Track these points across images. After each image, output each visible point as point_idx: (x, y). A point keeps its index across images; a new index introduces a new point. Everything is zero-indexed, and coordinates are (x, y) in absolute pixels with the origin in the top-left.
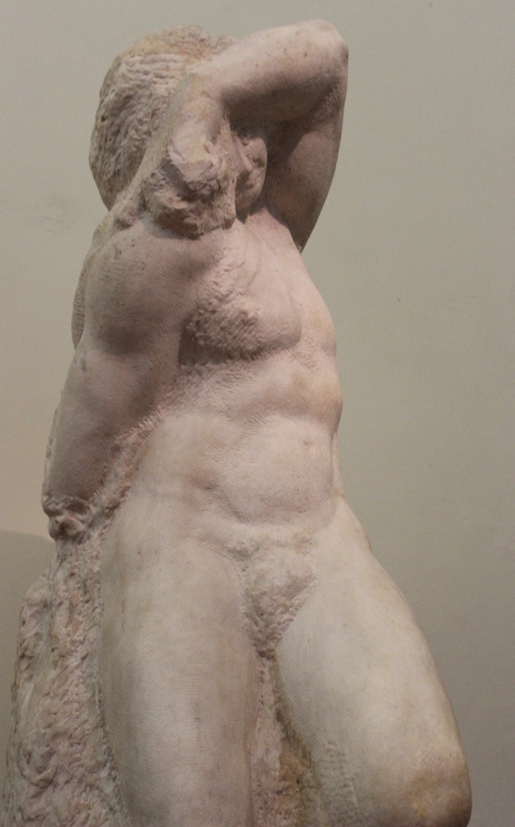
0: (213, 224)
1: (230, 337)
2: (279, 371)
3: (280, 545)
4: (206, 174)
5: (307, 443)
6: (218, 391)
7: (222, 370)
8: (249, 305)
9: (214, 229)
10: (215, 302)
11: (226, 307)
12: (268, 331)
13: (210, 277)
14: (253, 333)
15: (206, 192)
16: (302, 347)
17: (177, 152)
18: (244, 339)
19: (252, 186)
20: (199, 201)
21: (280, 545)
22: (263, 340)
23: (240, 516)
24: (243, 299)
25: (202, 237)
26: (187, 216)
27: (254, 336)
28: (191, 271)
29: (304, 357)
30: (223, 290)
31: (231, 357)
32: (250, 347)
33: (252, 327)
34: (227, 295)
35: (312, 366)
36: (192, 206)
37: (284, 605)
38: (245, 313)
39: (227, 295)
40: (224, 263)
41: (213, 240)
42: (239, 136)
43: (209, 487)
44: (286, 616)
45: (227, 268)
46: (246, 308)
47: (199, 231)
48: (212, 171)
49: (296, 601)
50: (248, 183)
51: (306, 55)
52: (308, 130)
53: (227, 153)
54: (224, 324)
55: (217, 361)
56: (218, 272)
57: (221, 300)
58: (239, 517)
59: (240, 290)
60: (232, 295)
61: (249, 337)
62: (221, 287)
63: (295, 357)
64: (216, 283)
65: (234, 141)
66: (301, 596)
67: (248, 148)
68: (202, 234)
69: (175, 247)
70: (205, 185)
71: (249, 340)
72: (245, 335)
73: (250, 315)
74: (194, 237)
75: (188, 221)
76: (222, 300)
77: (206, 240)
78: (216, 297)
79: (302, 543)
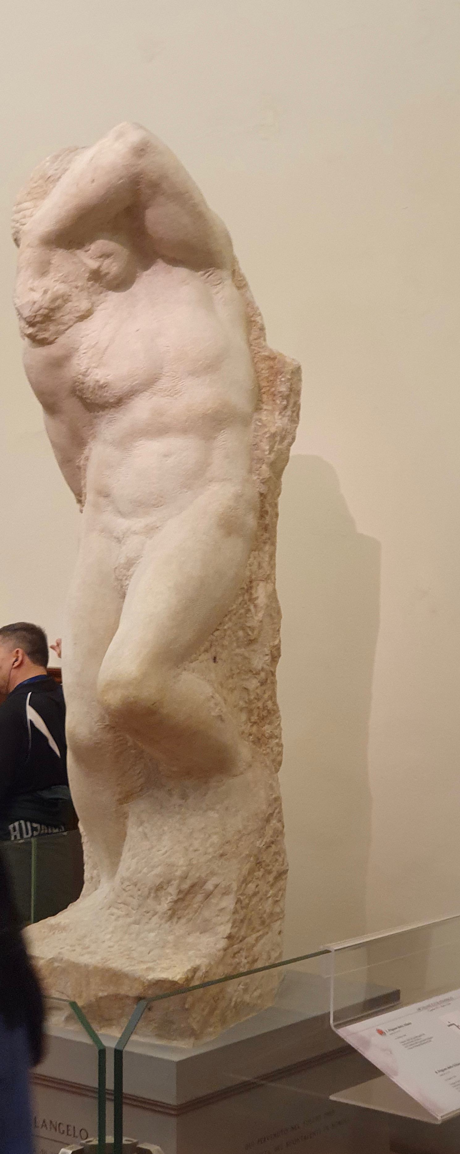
0: (63, 328)
1: (97, 396)
2: (141, 410)
3: (135, 533)
4: (33, 309)
5: (166, 456)
6: (110, 428)
7: (108, 415)
8: (99, 375)
9: (66, 330)
10: (80, 376)
11: (88, 379)
12: (119, 387)
13: (75, 361)
14: (110, 392)
15: (38, 319)
16: (164, 383)
17: (19, 298)
18: (105, 397)
19: (107, 274)
20: (38, 325)
21: (135, 533)
22: (118, 394)
23: (122, 514)
24: (97, 371)
25: (57, 340)
26: (36, 336)
27: (110, 393)
28: (59, 363)
29: (166, 390)
30: (83, 369)
31: (107, 407)
32: (112, 401)
33: (106, 388)
34: (87, 371)
35: (176, 394)
36: (36, 329)
37: (125, 575)
38: (98, 381)
39: (87, 371)
40: (82, 349)
41: (69, 337)
42: (78, 249)
43: (107, 496)
44: (127, 582)
45: (84, 351)
46: (98, 378)
47: (52, 339)
48: (36, 306)
49: (130, 573)
50: (103, 273)
51: (93, 181)
52: (145, 208)
53: (61, 275)
54: (91, 390)
55: (103, 411)
56: (79, 356)
57: (83, 375)
58: (121, 514)
59: (94, 365)
60: (90, 370)
61: (107, 394)
62: (81, 367)
63: (155, 394)
64: (78, 364)
65: (75, 255)
66: (132, 569)
67: (90, 252)
68: (56, 338)
69: (43, 351)
70: (35, 316)
71: (109, 396)
72: (105, 394)
73: (101, 382)
74: (51, 343)
75: (38, 338)
76: (84, 375)
77: (62, 340)
78: (80, 374)
79: (151, 530)
